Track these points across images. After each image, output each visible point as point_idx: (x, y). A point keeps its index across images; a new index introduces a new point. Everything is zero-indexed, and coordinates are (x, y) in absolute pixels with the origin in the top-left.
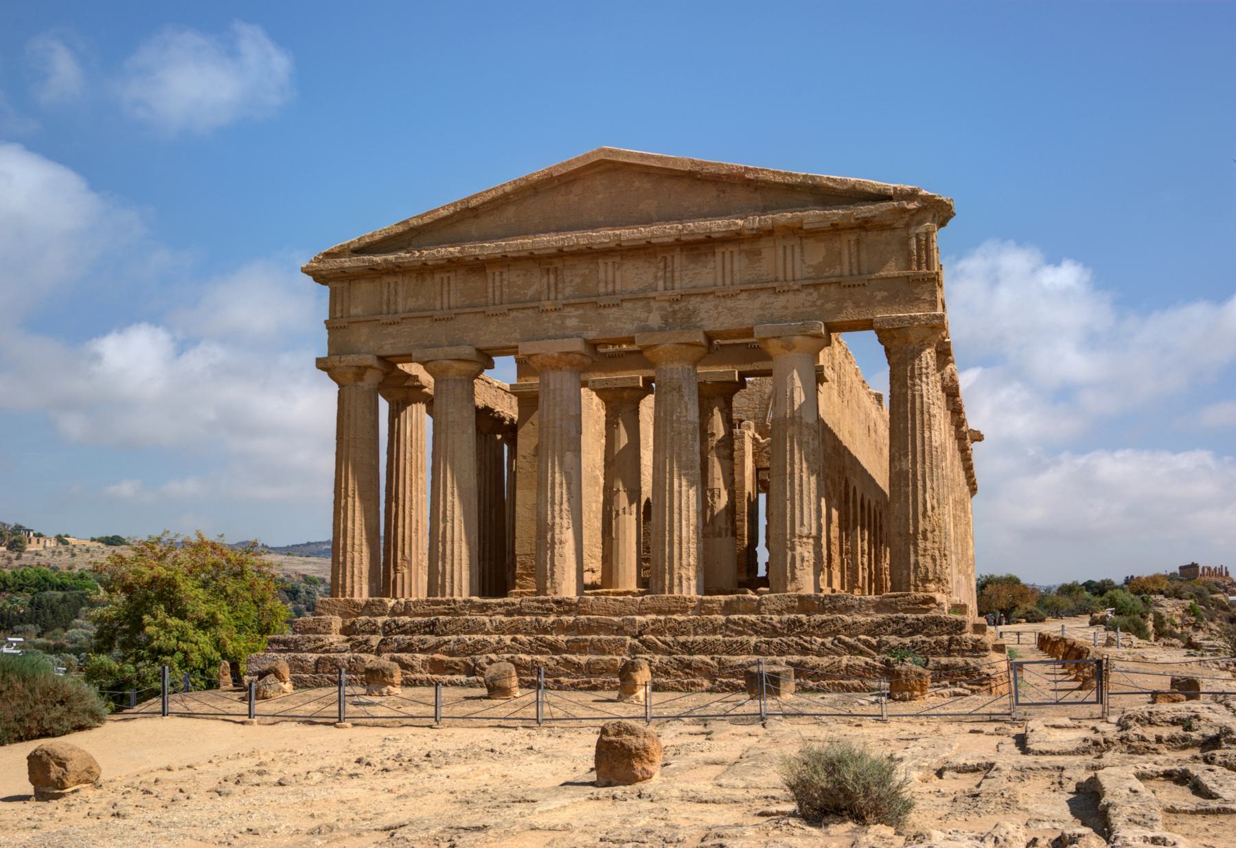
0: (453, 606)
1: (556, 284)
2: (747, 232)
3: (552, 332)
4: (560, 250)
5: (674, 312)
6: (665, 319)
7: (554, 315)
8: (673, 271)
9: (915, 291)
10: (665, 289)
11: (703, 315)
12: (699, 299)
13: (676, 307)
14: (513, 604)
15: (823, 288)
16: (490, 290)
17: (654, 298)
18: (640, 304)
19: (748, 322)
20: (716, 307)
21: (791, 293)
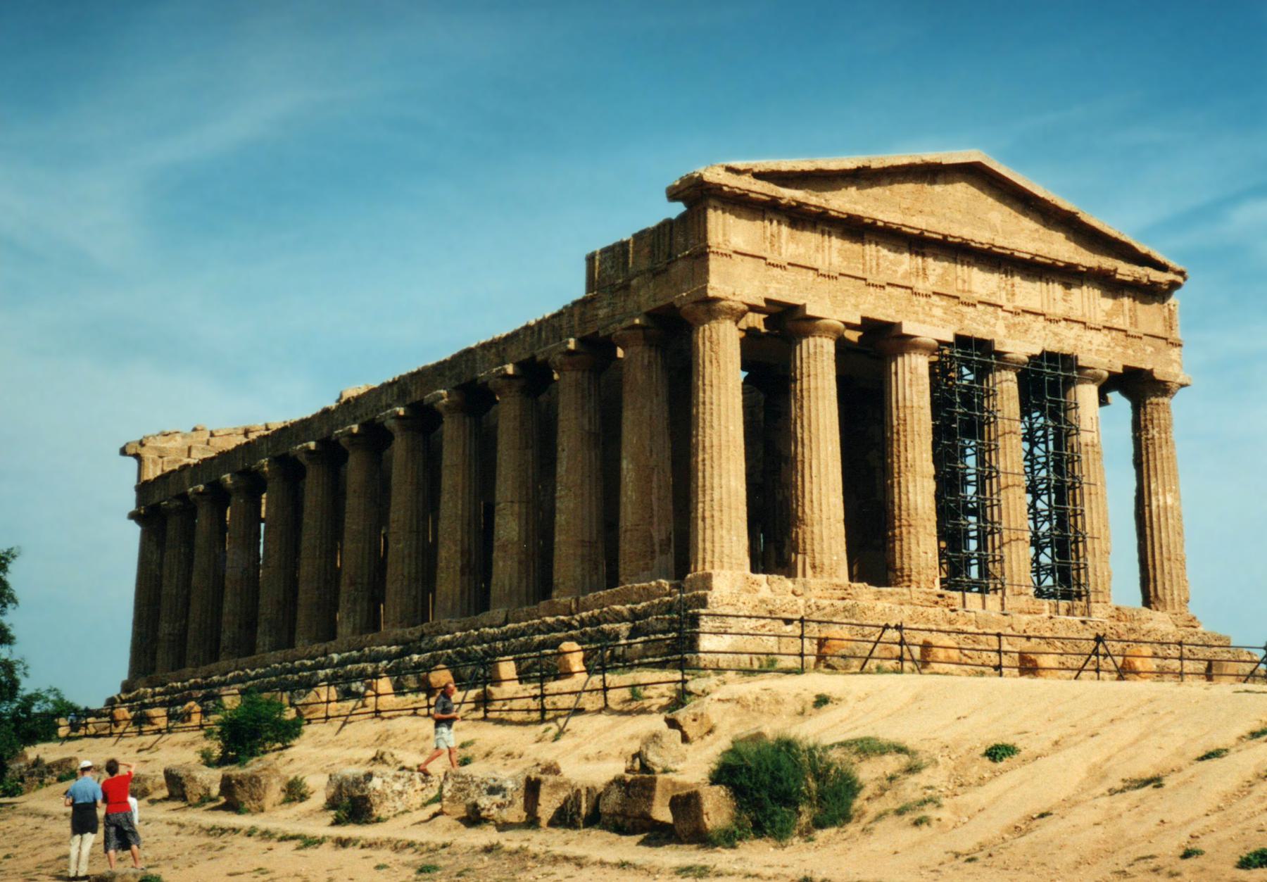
0: (849, 591)
1: (924, 269)
2: (1081, 269)
3: (921, 317)
4: (945, 237)
5: (1014, 325)
6: (1007, 327)
7: (923, 300)
8: (1013, 285)
9: (1171, 352)
10: (1008, 300)
11: (1035, 333)
12: (1032, 317)
13: (1017, 319)
14: (904, 594)
15: (1114, 333)
16: (867, 258)
17: (1001, 307)
18: (991, 309)
19: (1067, 350)
20: (1044, 328)
21: (1093, 332)
